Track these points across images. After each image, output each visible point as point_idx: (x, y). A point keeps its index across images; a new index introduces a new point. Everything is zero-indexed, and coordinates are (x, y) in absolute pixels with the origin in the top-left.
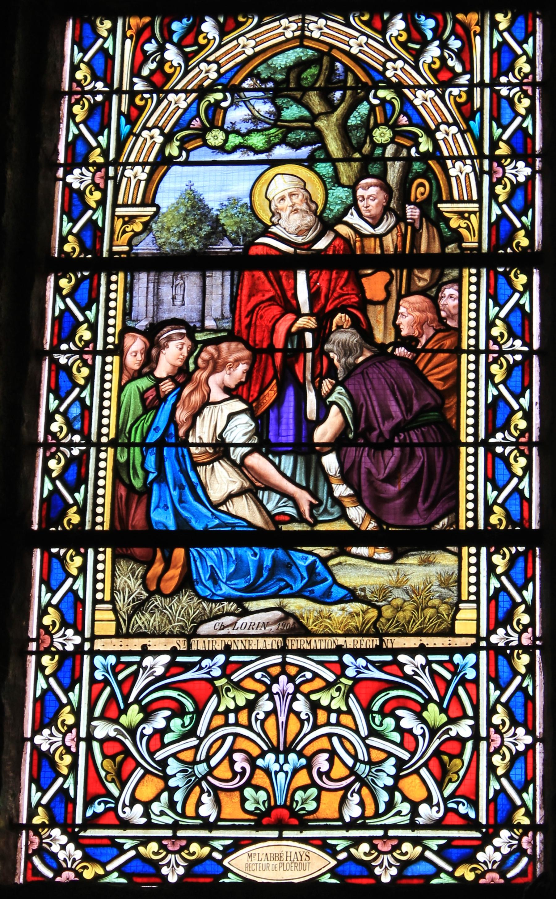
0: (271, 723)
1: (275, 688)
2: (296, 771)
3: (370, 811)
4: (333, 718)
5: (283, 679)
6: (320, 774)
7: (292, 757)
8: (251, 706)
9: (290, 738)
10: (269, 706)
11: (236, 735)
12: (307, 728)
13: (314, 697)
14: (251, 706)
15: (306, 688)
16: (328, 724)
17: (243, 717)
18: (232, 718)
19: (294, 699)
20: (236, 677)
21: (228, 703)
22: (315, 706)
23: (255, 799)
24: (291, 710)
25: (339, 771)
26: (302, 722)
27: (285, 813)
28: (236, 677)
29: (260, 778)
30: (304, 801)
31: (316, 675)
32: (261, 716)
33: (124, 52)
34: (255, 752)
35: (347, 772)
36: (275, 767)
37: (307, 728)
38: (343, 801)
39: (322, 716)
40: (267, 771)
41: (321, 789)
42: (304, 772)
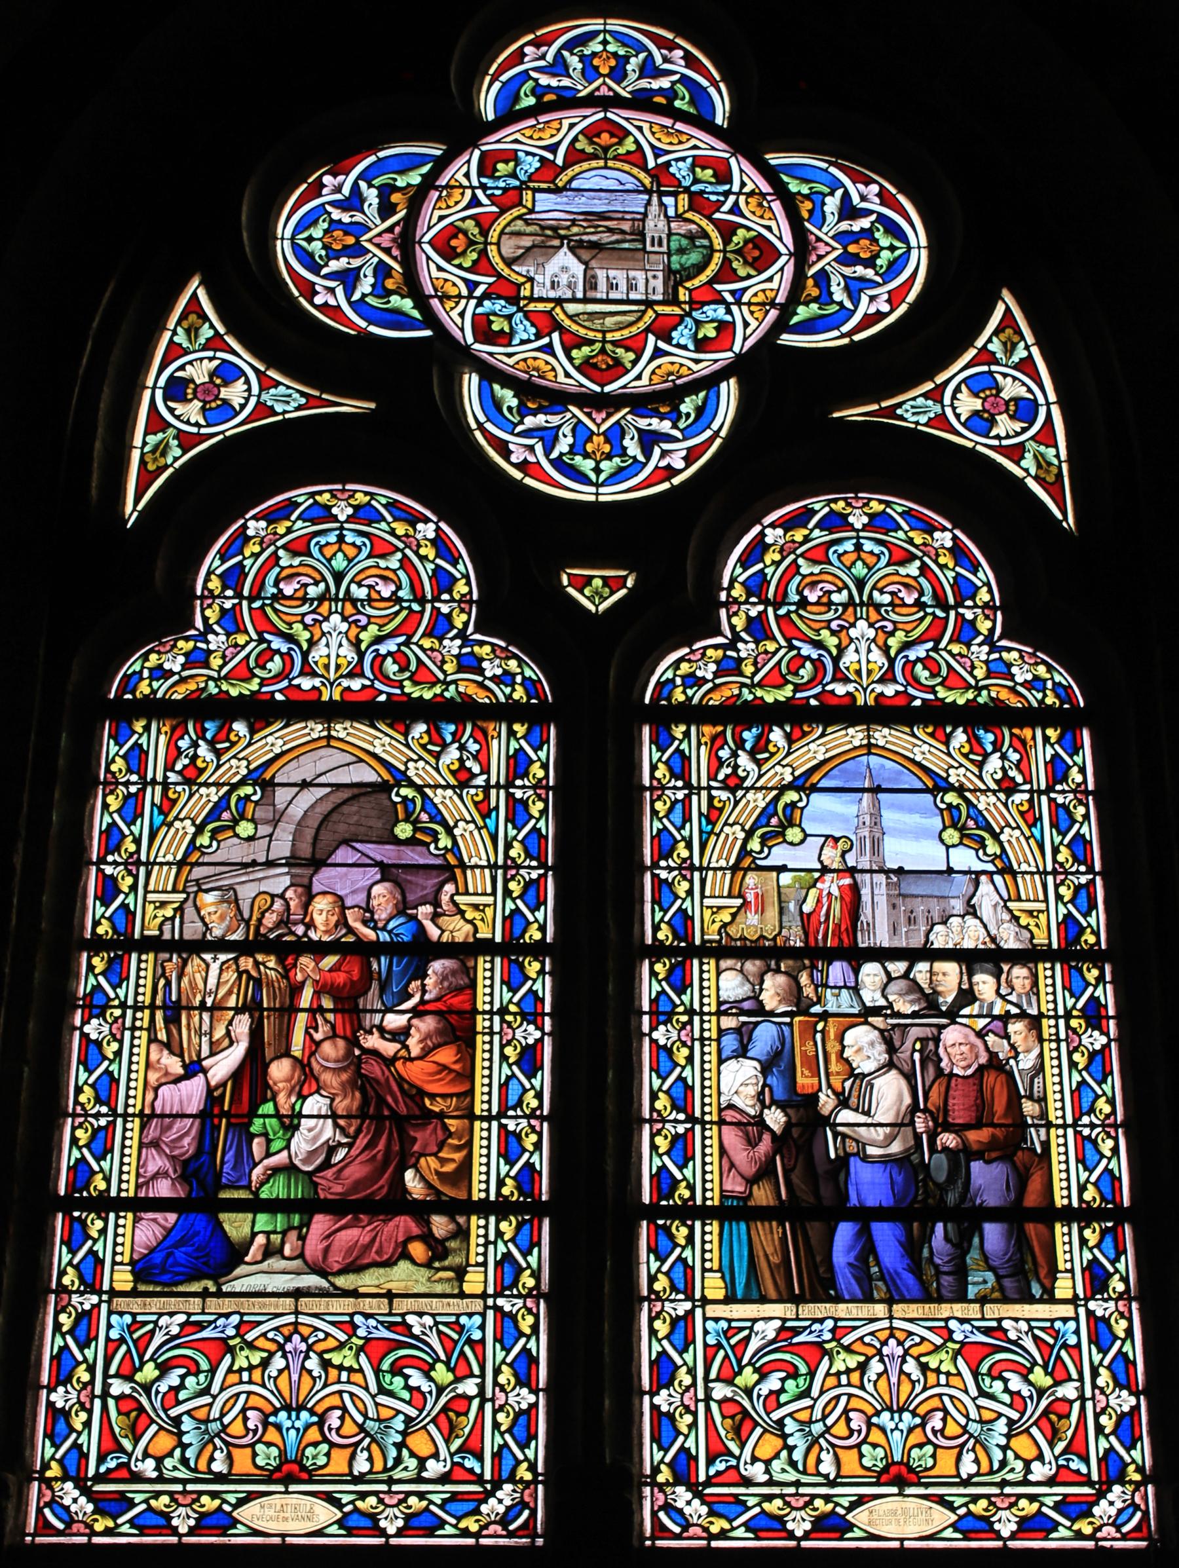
0: (883, 1383)
5: (892, 1342)
6: (934, 1432)
7: (907, 1416)
8: (863, 1367)
9: (903, 1398)
10: (879, 1368)
11: (850, 1396)
12: (918, 1388)
19: (904, 1361)
20: (846, 1341)
21: (839, 1366)
23: (873, 1457)
24: (901, 1372)
25: (952, 1429)
26: (913, 1383)
27: (904, 1469)
28: (846, 1341)
31: (923, 1339)
34: (870, 1411)
36: (890, 1425)
37: (918, 1388)
39: (932, 1378)
40: (883, 1430)
41: (936, 1447)
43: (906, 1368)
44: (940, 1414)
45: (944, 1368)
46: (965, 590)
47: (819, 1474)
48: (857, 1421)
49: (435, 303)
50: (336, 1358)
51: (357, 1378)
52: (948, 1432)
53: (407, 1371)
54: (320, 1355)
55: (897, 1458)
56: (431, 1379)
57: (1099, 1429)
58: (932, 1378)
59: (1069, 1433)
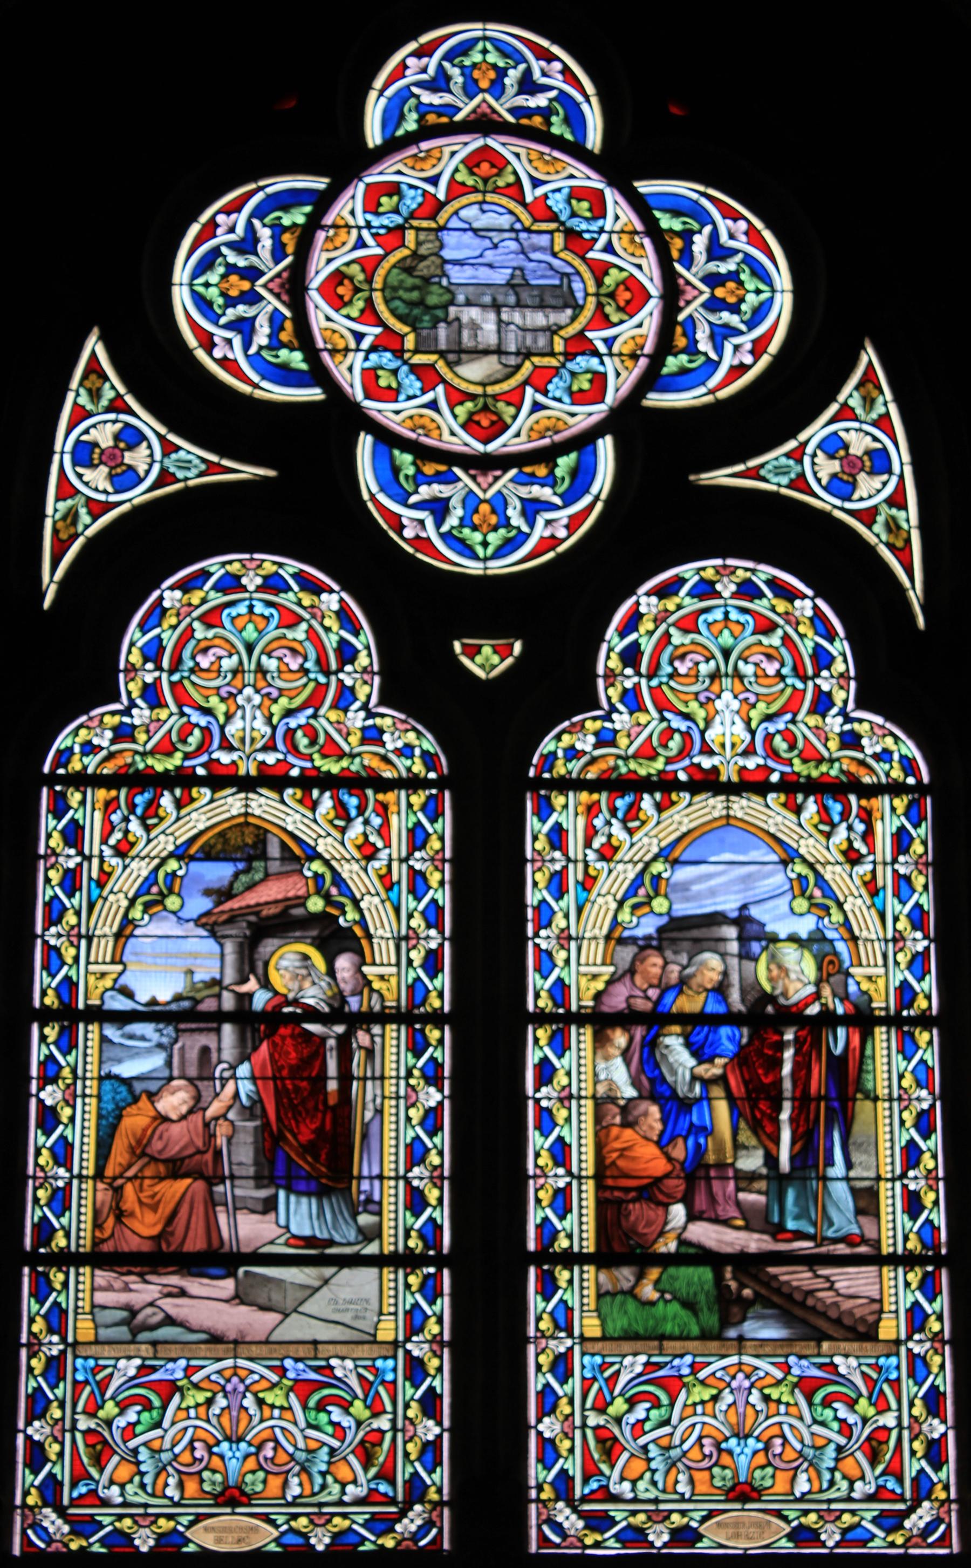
3: (816, 1487)
4: (782, 1409)
13: (767, 1391)
14: (715, 1399)
15: (759, 1384)
16: (778, 1414)
17: (709, 1406)
18: (699, 1409)
22: (766, 1399)
29: (726, 1459)
30: (763, 1478)
32: (724, 1408)
33: (575, 827)
35: (794, 1455)
38: (794, 1479)
42: (762, 1454)
44: (778, 1441)
45: (784, 1399)
46: (822, 659)
49: (326, 356)
50: (269, 1398)
51: (288, 1415)
52: (786, 1457)
53: (329, 1408)
54: (255, 1394)
56: (349, 1414)
57: (913, 1453)
59: (888, 1457)
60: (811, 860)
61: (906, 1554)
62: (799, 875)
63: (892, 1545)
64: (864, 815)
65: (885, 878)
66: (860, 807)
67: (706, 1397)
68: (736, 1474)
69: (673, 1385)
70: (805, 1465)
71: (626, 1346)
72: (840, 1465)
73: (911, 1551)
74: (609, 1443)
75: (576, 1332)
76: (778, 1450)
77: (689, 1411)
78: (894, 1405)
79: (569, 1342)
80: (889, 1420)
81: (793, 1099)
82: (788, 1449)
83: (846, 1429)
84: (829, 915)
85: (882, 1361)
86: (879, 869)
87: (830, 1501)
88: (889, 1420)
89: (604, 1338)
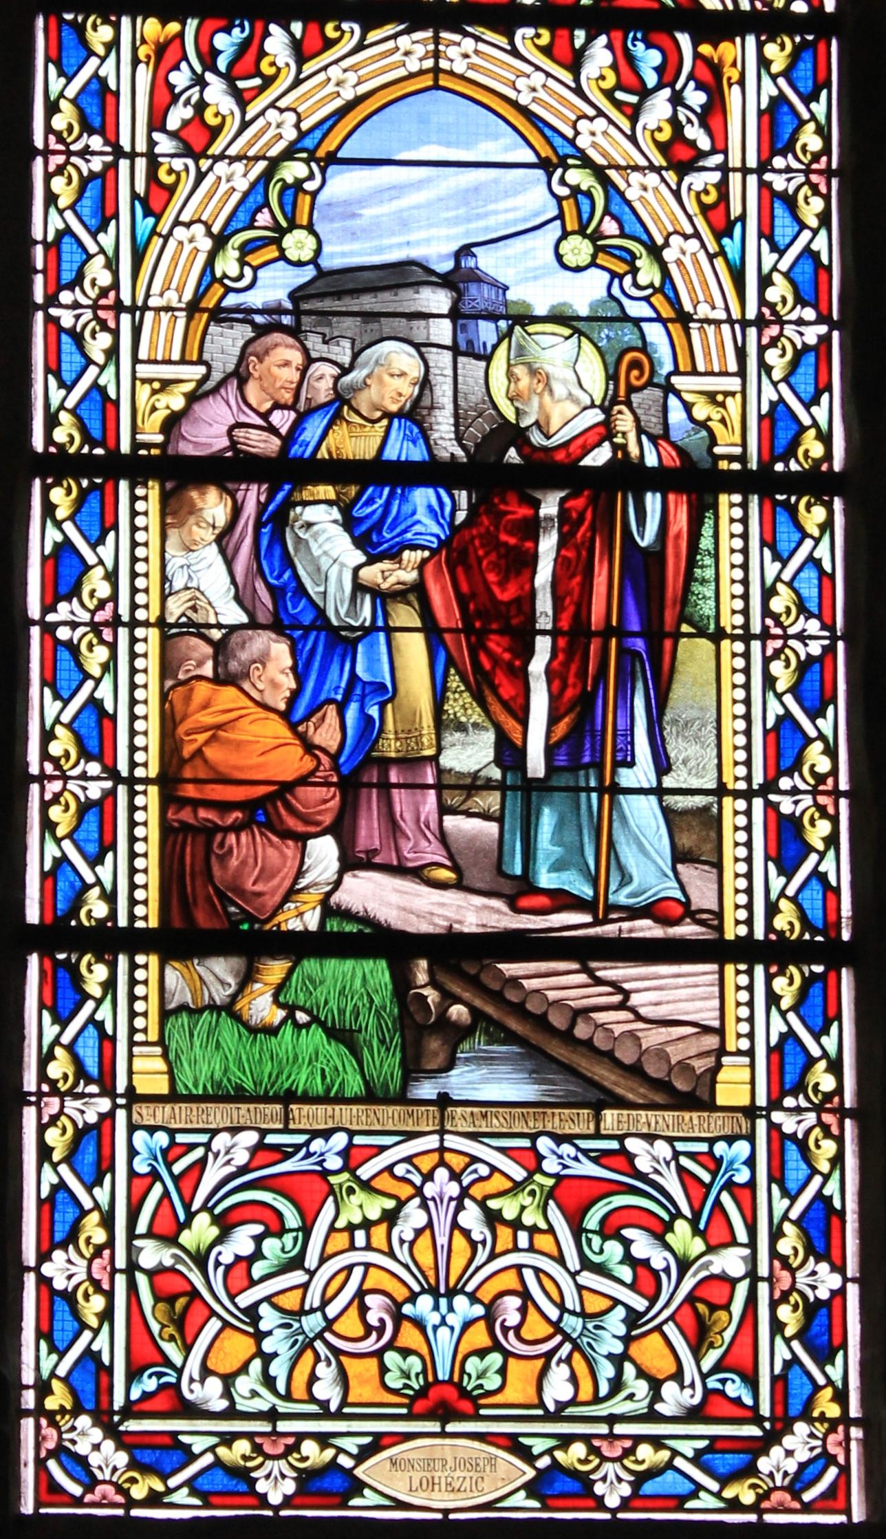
1: (429, 1190)
2: (467, 1325)
6: (505, 1330)
7: (460, 1302)
8: (390, 1218)
14: (390, 1218)
19: (460, 1208)
24: (455, 1225)
27: (451, 1394)
36: (433, 1319)
39: (504, 1233)
40: (419, 1324)
41: (507, 1354)
43: (463, 1219)
47: (312, 1399)
48: (377, 1308)
55: (443, 1375)
58: (504, 1233)
60: (601, 161)
61: (761, 1525)
62: (576, 191)
63: (734, 1505)
64: (705, 74)
65: (745, 197)
66: (697, 56)
67: (374, 1215)
68: (429, 1363)
69: (310, 1192)
70: (567, 1347)
71: (218, 1115)
72: (634, 1350)
73: (769, 1518)
74: (181, 1303)
75: (121, 1087)
76: (513, 1319)
77: (341, 1240)
78: (742, 1235)
79: (104, 1104)
80: (731, 1262)
81: (554, 633)
82: (532, 1314)
83: (645, 1277)
84: (634, 271)
85: (720, 1148)
86: (735, 179)
87: (612, 1419)
88: (731, 1262)
89: (173, 1097)
